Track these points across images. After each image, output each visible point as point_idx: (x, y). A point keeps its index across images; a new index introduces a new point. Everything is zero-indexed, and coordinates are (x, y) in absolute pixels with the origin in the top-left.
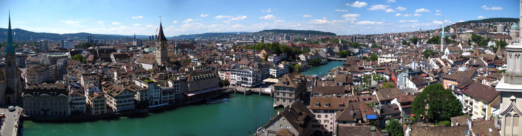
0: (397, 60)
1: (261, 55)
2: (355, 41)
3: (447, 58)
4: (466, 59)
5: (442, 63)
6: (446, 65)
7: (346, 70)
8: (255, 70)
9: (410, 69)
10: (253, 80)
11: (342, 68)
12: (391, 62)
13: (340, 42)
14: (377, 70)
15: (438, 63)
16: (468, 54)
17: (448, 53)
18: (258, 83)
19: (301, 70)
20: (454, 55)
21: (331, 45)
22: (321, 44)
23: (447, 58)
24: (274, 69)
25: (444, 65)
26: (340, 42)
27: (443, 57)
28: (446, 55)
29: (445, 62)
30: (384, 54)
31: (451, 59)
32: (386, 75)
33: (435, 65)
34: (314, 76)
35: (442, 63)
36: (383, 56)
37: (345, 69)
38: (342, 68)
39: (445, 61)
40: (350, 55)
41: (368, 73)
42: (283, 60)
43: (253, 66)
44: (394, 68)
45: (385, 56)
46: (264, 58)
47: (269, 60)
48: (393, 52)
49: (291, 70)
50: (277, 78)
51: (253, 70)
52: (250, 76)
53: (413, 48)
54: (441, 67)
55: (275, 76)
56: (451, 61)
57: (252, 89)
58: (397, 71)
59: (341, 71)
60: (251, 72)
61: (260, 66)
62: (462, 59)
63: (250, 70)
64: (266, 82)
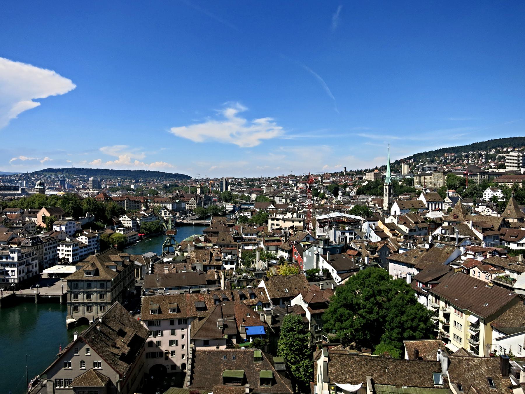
0: (302, 224)
1: (38, 220)
2: (226, 189)
3: (395, 221)
4: (436, 224)
5: (387, 231)
6: (395, 235)
7: (209, 242)
8: (23, 250)
9: (327, 241)
10: (19, 273)
11: (202, 239)
12: (292, 227)
13: (199, 191)
14: (267, 241)
15: (378, 231)
16: (439, 215)
17: (398, 213)
18: (30, 280)
19: (123, 245)
20: (409, 215)
21: (182, 196)
22: (162, 194)
23: (395, 221)
24: (68, 245)
25: (390, 235)
26: (199, 191)
27: (388, 221)
28: (394, 216)
29: (391, 230)
30: (279, 213)
31: (405, 224)
32: (283, 250)
33: (372, 233)
34: (150, 254)
35: (387, 231)
36: (278, 216)
37: (207, 240)
38: (202, 239)
39: (392, 227)
40: (218, 215)
41: (250, 248)
42: (86, 226)
43: (19, 244)
44: (297, 238)
45: (281, 217)
46: (44, 226)
47: (56, 228)
48: (293, 211)
49: (103, 246)
50: (73, 264)
51: (19, 252)
52: (13, 265)
53: (331, 203)
54: (384, 238)
55: (71, 260)
56: (405, 229)
57: (18, 293)
58: (302, 244)
59: (200, 244)
60: (15, 256)
61: (36, 242)
62: (426, 225)
63: (13, 252)
64: (50, 275)
